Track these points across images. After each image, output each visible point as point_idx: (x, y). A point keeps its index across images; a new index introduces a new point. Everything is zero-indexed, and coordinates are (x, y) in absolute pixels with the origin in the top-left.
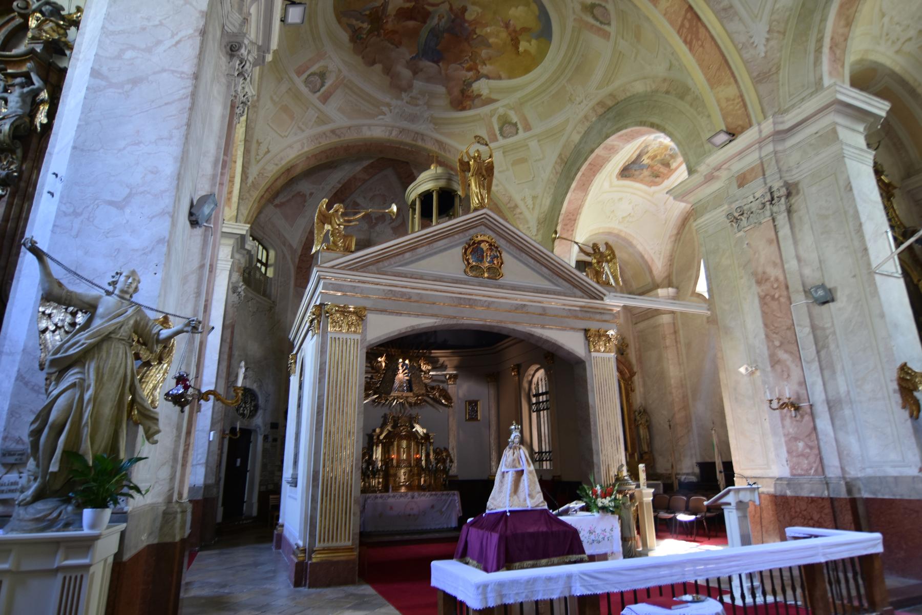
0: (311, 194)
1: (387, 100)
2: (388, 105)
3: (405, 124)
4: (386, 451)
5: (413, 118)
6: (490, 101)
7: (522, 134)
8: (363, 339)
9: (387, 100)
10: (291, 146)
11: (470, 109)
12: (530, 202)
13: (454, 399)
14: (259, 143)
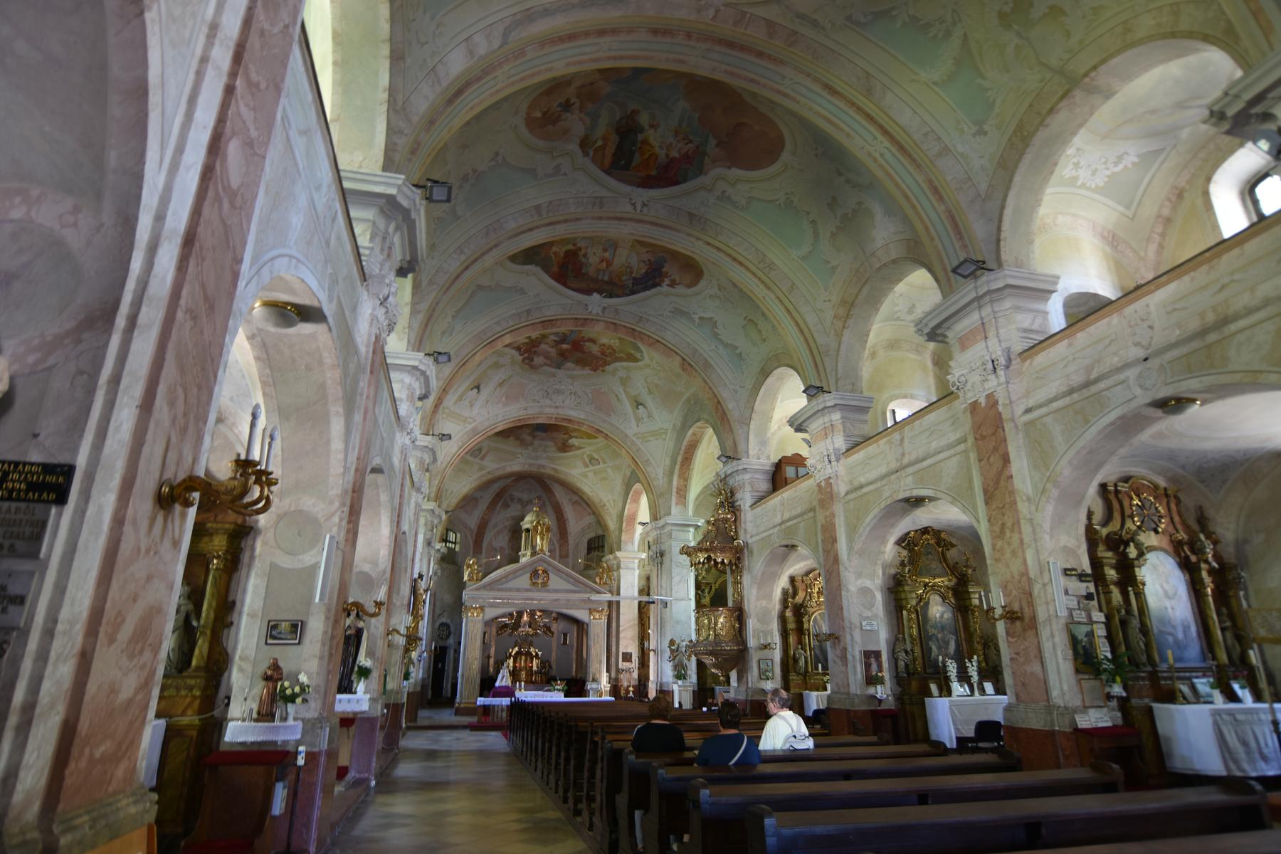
0: (481, 497)
1: (520, 451)
2: (521, 453)
3: (532, 461)
4: (515, 662)
5: (537, 458)
6: (579, 448)
7: (602, 465)
8: (483, 619)
9: (520, 451)
10: (464, 486)
11: (570, 451)
12: (611, 501)
13: (556, 632)
14: (446, 490)
